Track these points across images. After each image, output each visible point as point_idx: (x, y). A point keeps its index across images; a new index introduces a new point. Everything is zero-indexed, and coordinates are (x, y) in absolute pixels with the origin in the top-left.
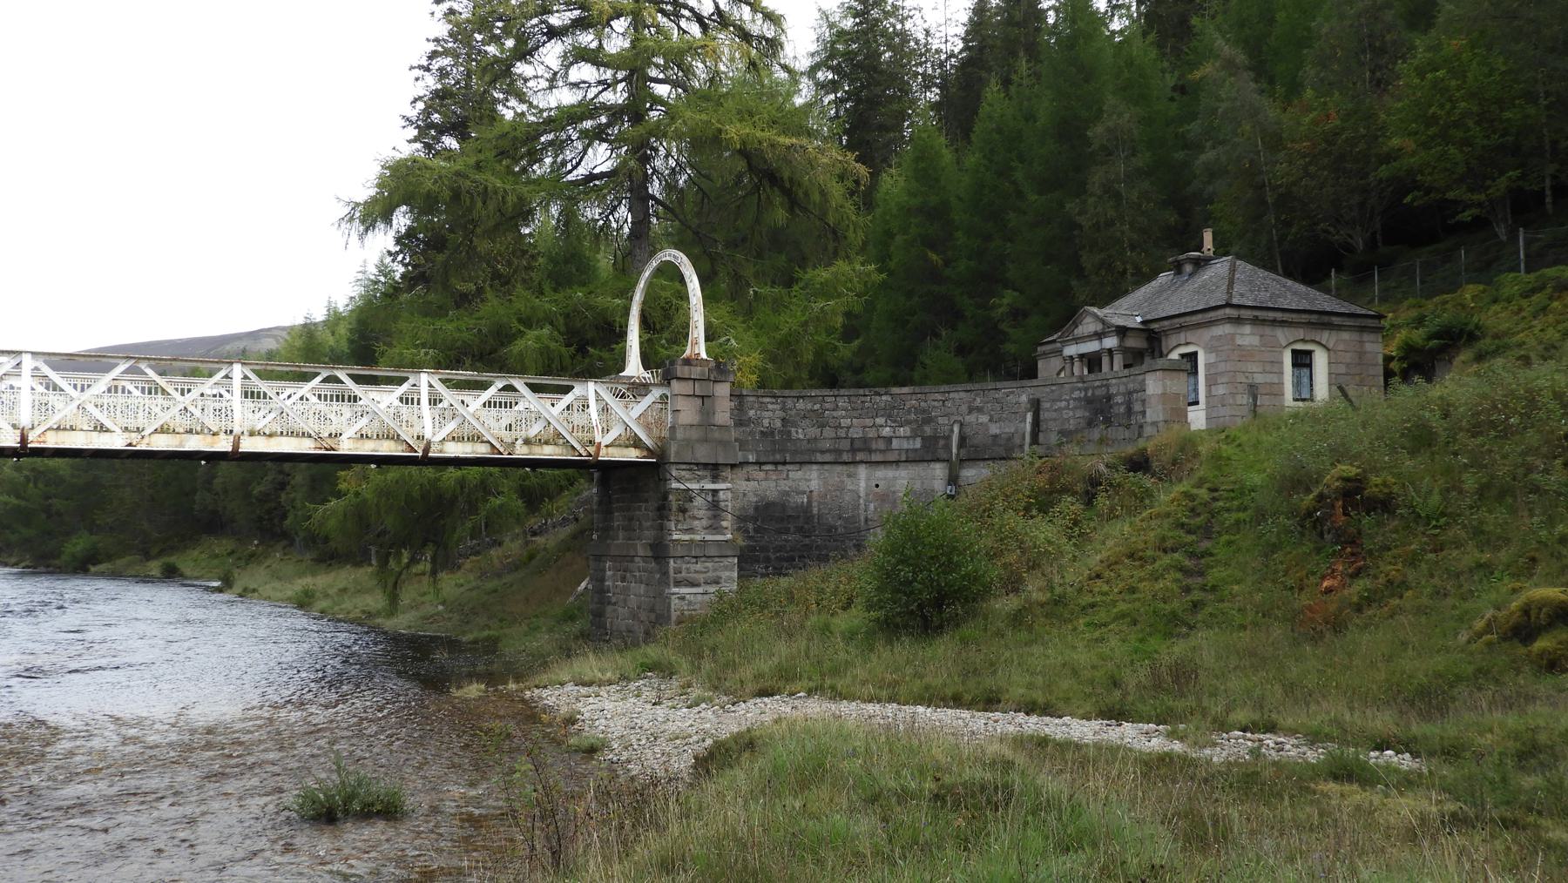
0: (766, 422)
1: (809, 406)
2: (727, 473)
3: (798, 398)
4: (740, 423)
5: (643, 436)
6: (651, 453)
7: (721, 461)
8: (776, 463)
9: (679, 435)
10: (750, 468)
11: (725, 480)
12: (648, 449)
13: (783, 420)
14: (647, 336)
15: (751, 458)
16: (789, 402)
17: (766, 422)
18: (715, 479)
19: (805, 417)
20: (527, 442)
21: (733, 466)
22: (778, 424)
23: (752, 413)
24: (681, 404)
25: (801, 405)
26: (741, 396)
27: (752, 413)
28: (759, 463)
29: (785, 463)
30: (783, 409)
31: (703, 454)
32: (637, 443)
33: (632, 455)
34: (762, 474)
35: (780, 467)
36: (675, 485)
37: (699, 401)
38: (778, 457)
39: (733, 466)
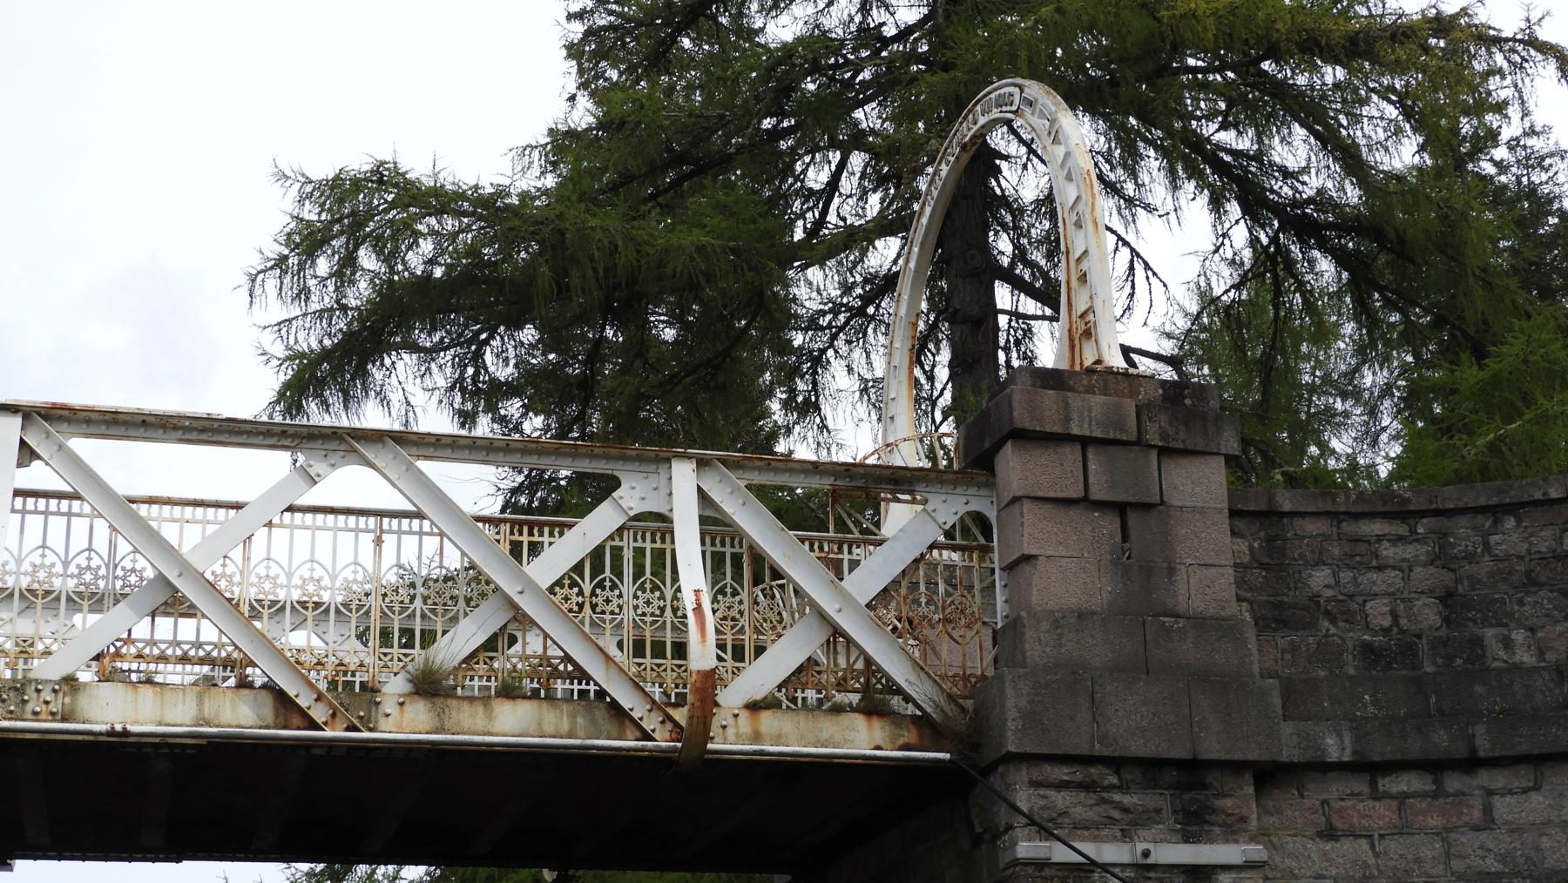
0: (1379, 613)
1: (1544, 540)
2: (1241, 798)
3: (1497, 512)
4: (1276, 618)
5: (897, 669)
6: (927, 728)
7: (1212, 749)
8: (1435, 766)
9: (1037, 648)
10: (1335, 788)
11: (1233, 830)
13: (1446, 598)
15: (1335, 748)
16: (1464, 534)
17: (1379, 613)
18: (1194, 825)
19: (1531, 582)
20: (429, 686)
21: (1270, 776)
22: (1428, 615)
23: (1319, 579)
24: (1035, 532)
25: (1510, 537)
26: (1270, 516)
27: (1319, 579)
28: (1367, 768)
29: (1471, 763)
30: (1442, 557)
31: (1134, 723)
32: (876, 698)
33: (861, 739)
34: (1383, 813)
35: (1454, 782)
36: (1027, 847)
37: (1109, 526)
38: (1442, 740)
39: (1270, 776)
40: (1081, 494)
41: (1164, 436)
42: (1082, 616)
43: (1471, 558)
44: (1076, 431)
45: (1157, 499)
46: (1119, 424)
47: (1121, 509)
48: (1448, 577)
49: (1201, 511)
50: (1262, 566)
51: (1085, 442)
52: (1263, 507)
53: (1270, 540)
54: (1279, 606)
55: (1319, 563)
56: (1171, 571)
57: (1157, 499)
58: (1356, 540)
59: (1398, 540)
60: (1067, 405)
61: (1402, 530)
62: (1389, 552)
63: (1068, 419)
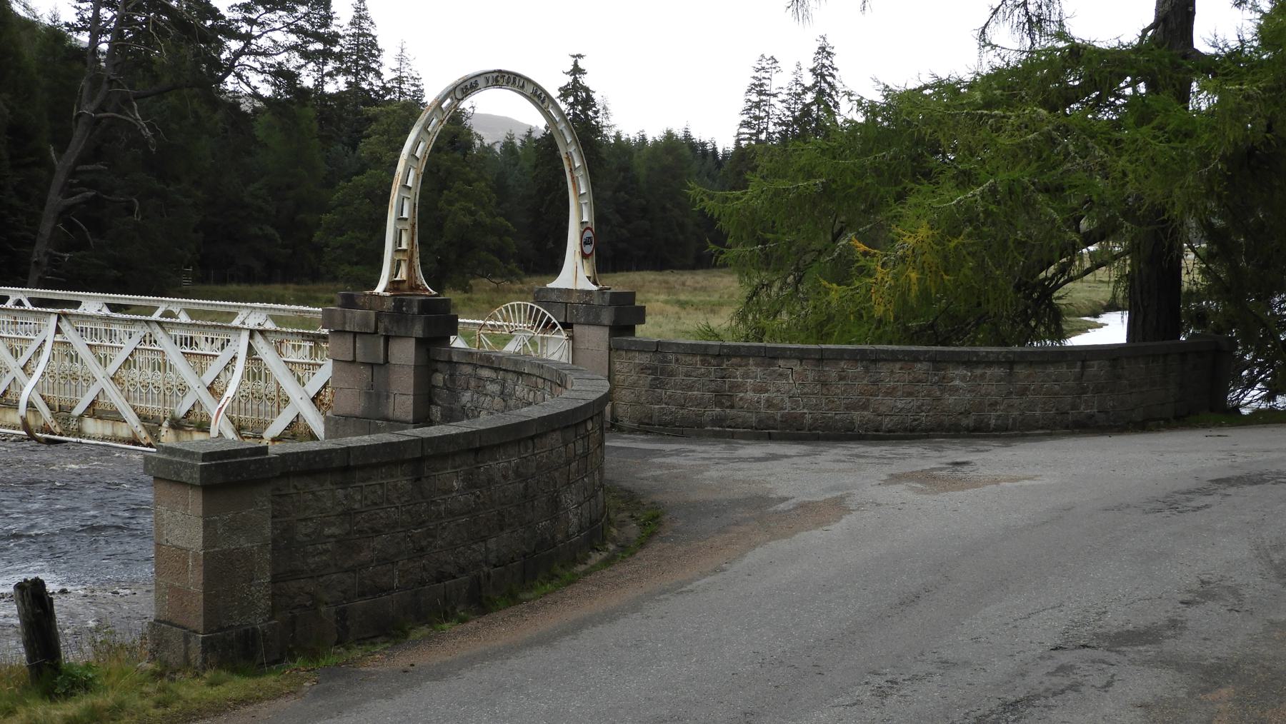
12: (616, 426)
14: (34, 275)
37: (366, 373)
40: (351, 359)
41: (386, 330)
42: (346, 417)
43: (510, 395)
44: (348, 329)
45: (381, 361)
46: (367, 325)
47: (372, 365)
48: (503, 404)
49: (402, 366)
50: (448, 389)
51: (355, 334)
52: (446, 359)
53: (451, 375)
54: (451, 410)
55: (468, 388)
56: (388, 397)
57: (381, 361)
58: (480, 379)
59: (493, 381)
60: (344, 316)
61: (493, 375)
62: (492, 388)
63: (345, 323)
